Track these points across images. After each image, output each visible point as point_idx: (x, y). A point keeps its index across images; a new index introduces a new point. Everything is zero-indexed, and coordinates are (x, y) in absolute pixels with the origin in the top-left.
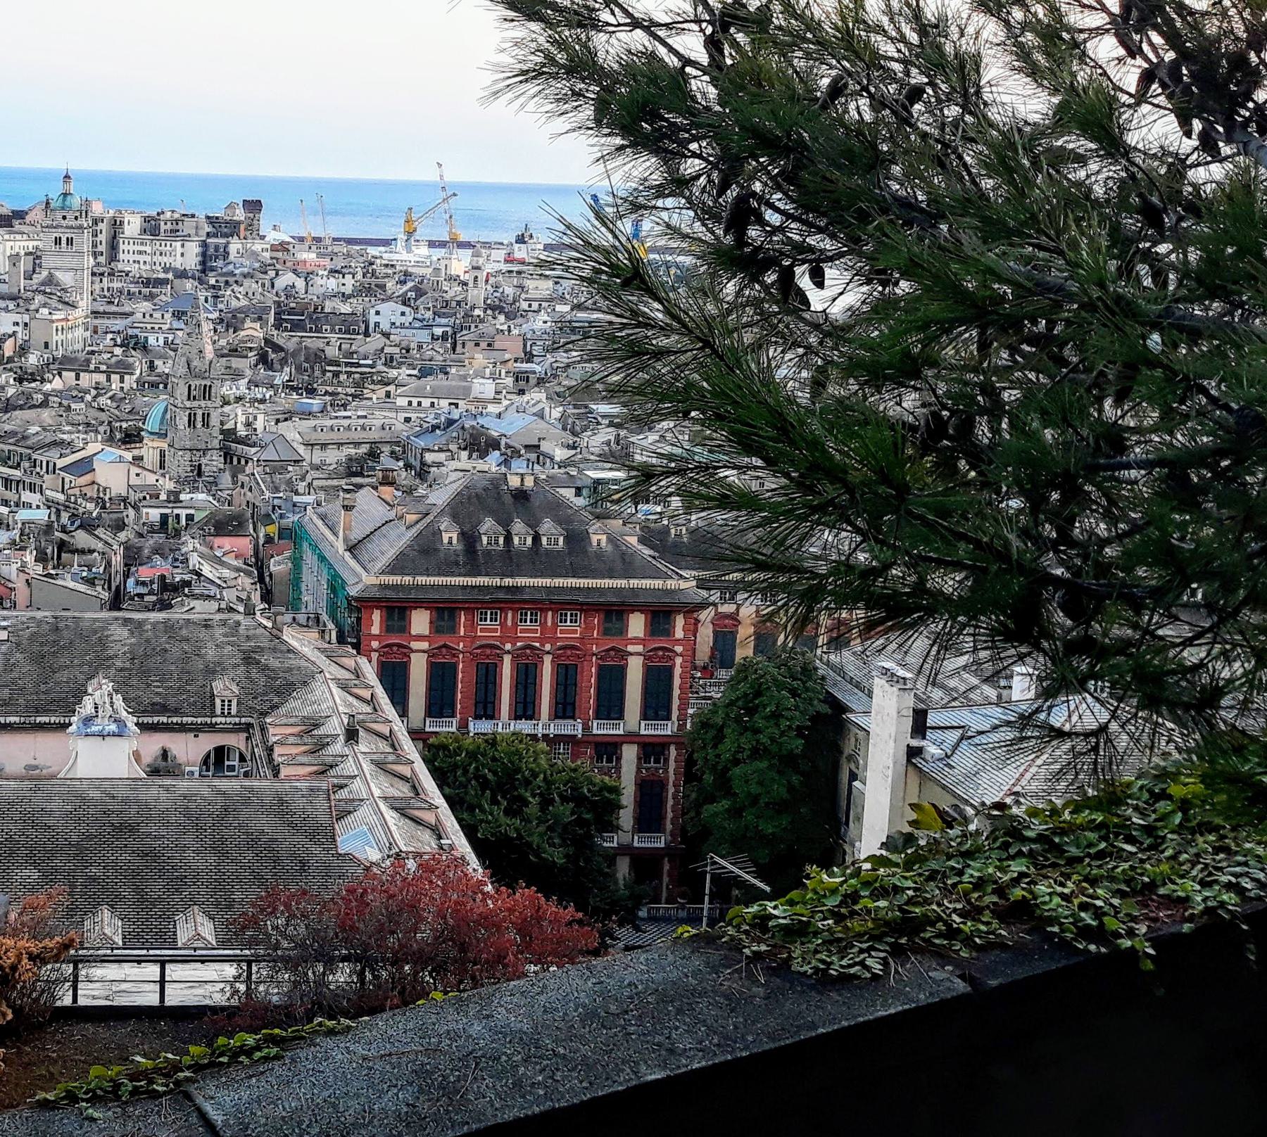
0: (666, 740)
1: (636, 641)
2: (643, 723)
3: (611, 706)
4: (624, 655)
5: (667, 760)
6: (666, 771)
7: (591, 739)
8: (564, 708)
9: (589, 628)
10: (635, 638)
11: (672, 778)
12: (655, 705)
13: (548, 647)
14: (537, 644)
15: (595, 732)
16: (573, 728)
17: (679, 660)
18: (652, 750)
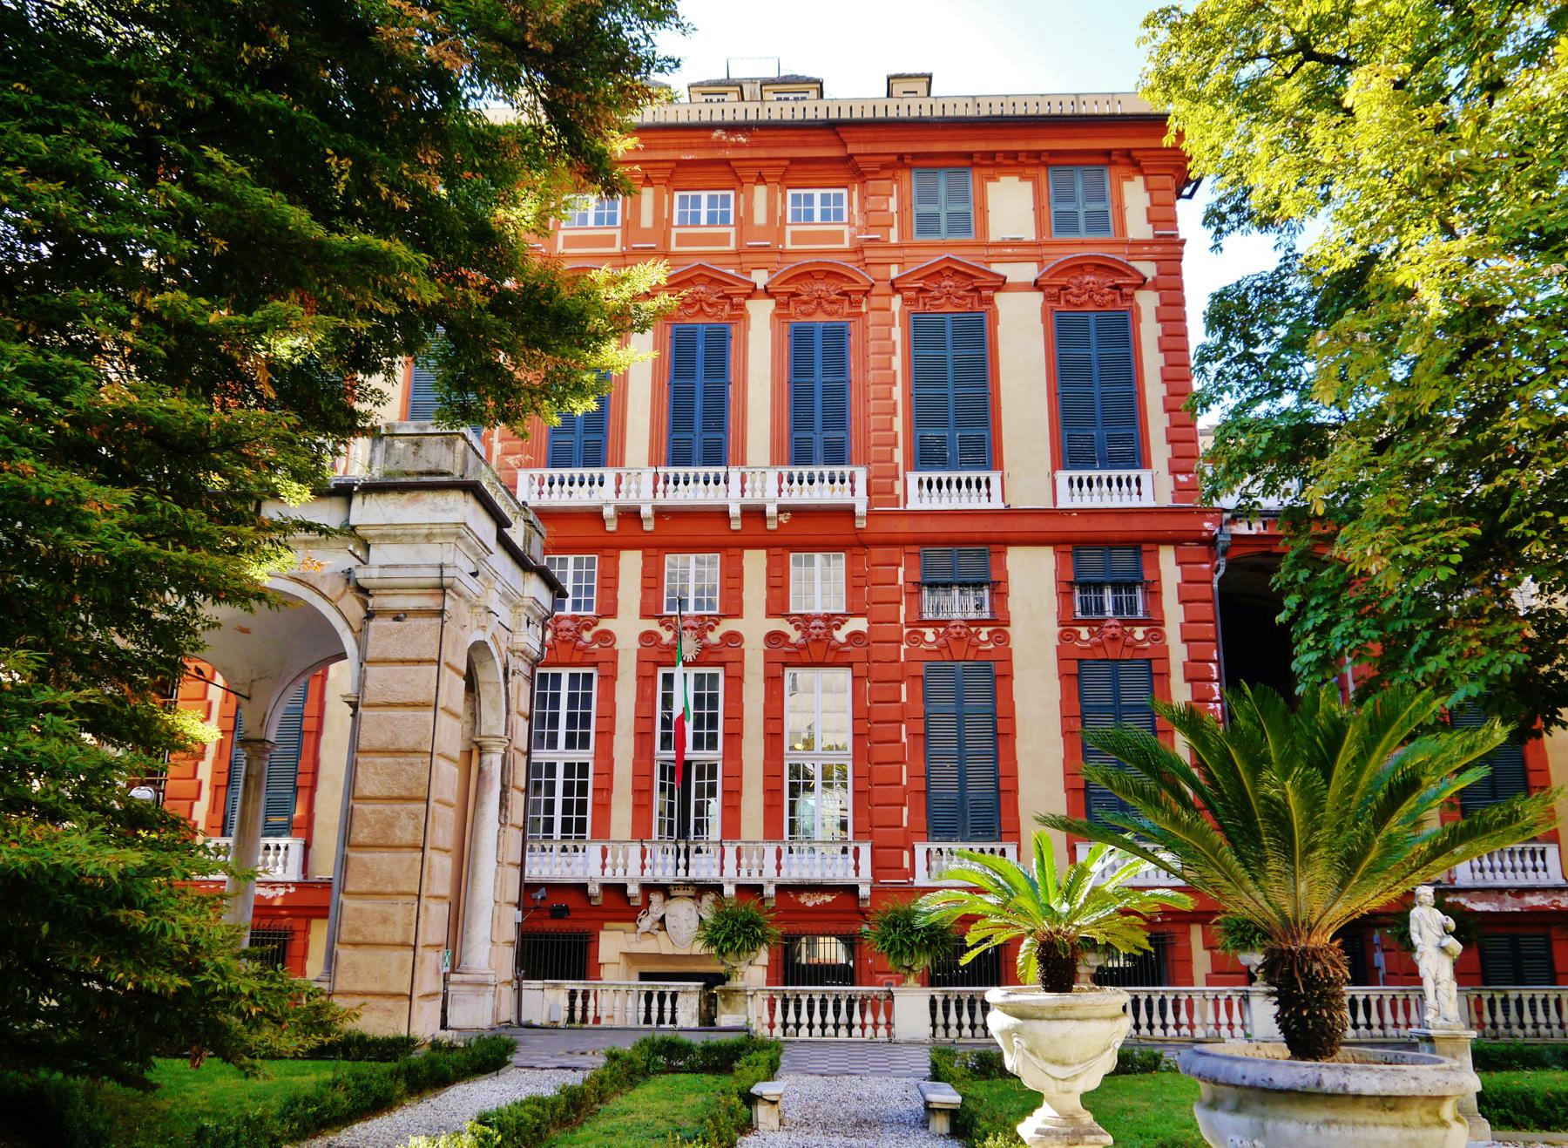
0: (1137, 524)
1: (1016, 249)
2: (1063, 476)
3: (959, 427)
4: (982, 288)
5: (1154, 592)
6: (1155, 624)
7: (903, 527)
8: (816, 429)
9: (873, 219)
10: (1016, 243)
11: (1178, 654)
12: (1095, 425)
13: (760, 278)
14: (732, 272)
15: (913, 505)
16: (841, 489)
17: (1147, 302)
18: (1103, 560)
